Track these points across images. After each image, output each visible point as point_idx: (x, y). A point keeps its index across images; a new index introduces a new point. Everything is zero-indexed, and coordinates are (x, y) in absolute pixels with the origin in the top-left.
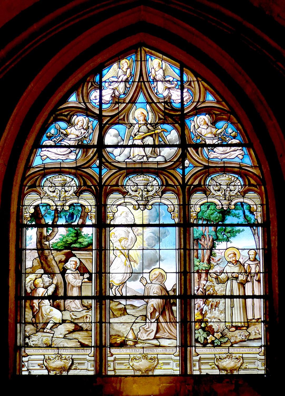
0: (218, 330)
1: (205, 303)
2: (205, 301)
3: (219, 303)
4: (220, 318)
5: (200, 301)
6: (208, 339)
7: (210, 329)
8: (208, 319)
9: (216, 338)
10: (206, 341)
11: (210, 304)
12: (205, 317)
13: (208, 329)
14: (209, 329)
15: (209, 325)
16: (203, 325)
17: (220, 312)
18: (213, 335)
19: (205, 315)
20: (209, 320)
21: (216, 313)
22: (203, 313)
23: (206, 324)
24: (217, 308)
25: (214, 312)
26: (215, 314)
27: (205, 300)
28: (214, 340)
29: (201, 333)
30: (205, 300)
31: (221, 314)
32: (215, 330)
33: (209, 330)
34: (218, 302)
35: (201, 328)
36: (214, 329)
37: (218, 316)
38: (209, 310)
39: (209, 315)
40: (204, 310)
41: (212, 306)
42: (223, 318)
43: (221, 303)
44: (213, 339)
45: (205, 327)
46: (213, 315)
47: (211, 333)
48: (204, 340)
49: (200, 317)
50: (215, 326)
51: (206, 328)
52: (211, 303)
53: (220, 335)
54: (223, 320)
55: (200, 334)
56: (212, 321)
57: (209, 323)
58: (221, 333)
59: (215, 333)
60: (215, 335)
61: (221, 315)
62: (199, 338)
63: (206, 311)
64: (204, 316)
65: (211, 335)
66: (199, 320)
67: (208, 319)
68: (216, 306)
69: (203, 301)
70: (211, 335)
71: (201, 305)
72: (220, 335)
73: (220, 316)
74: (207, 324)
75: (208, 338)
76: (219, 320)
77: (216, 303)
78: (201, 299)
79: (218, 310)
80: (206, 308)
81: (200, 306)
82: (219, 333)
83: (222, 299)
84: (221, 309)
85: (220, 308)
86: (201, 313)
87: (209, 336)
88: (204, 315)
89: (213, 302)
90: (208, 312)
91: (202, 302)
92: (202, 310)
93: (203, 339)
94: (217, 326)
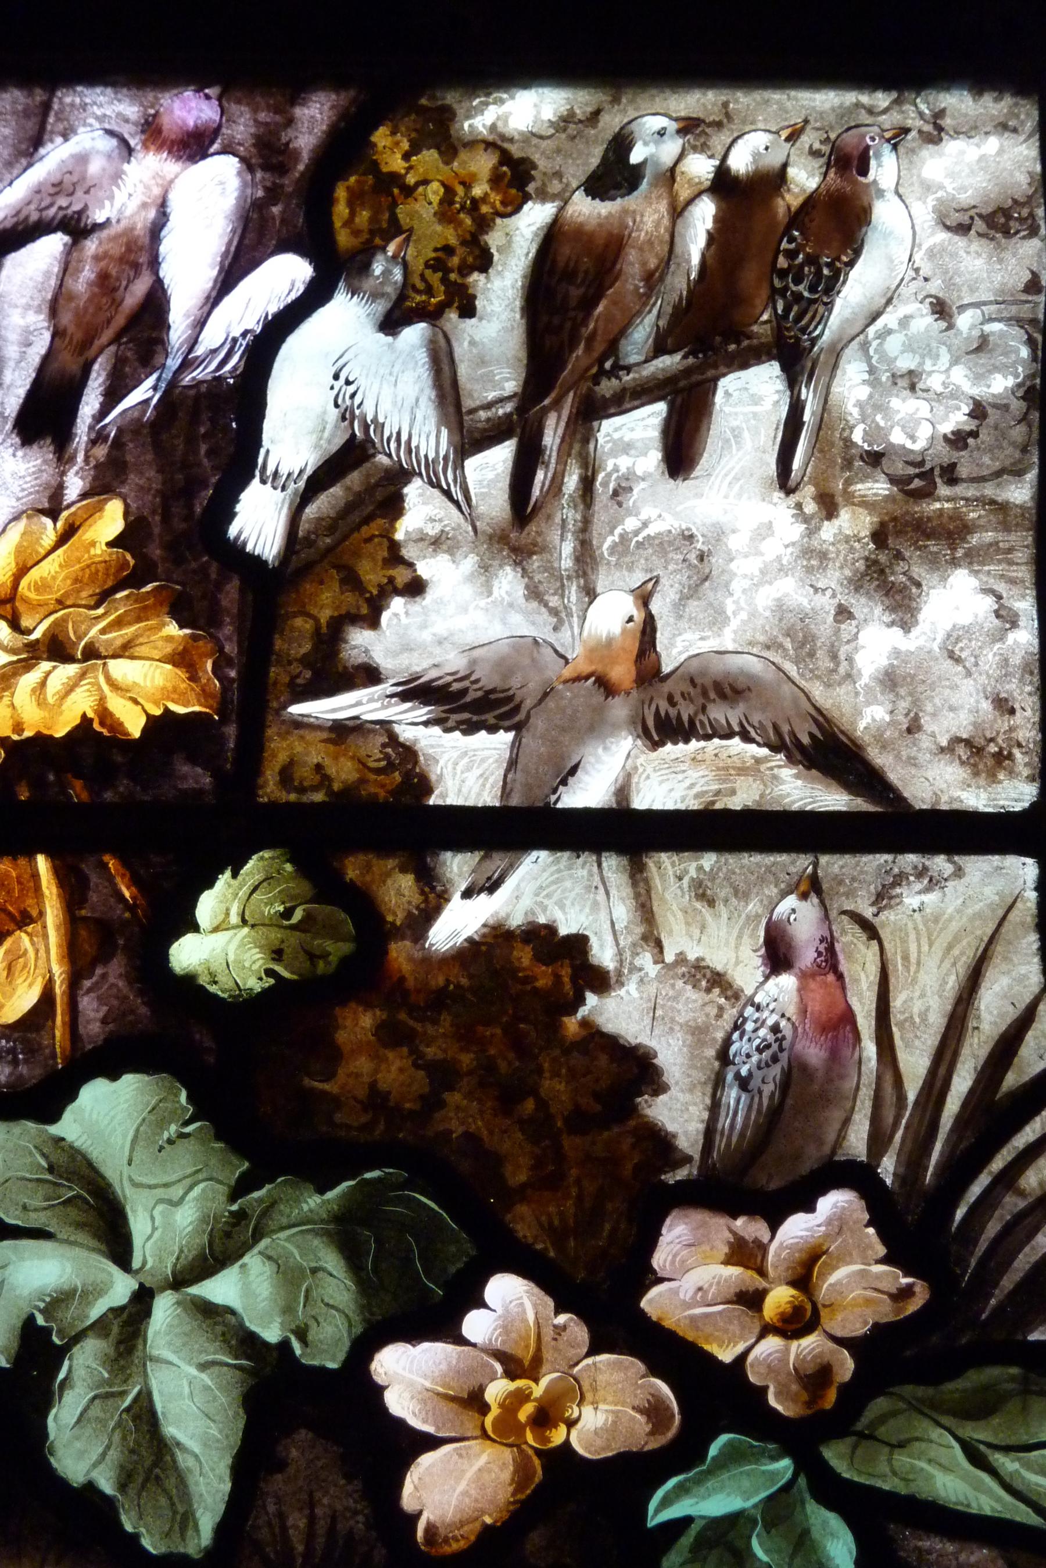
0: (798, 1092)
1: (304, 214)
2: (345, 147)
3: (840, 220)
4: (869, 717)
5: (150, 167)
6: (399, 1403)
7: (507, 1094)
8: (412, 724)
9: (710, 1397)
10: (315, 1488)
11: (535, 216)
12: (336, 675)
13: (395, 1073)
14: (443, 1076)
15: (458, 923)
16: (223, 941)
17: (852, 524)
18: (607, 1300)
19: (327, 600)
20: (467, 768)
21: (721, 532)
22: (260, 520)
23: (363, 907)
24: (750, 399)
25: (659, 508)
26: (698, 560)
27: (313, 118)
28: (633, 1473)
29: (165, 1220)
30: (313, 118)
31: (886, 574)
32: (679, 1113)
33: (462, 1114)
34: (805, 178)
35: (173, 1033)
36: (639, 1070)
37: (799, 637)
38: (471, 441)
39: (454, 611)
40: (293, 432)
41: (568, 287)
42: (960, 706)
43: (886, 213)
44: (609, 1409)
45: (285, 1016)
46: (611, 614)
47: (525, 1224)
48: (251, 1465)
49: (141, 681)
50: (683, 980)
51: (359, 1024)
52: (535, 216)
53: (863, 1284)
54: (981, 755)
55: (117, 1245)
56: (588, 792)
57: (458, 866)
58: (910, 1226)
59: (676, 1235)
60: (690, 1271)
61: (902, 604)
62: (84, 1364)
63: (360, 476)
64: (296, 641)
65: (508, 1294)
66: (92, 745)
67: (412, 724)
68: (713, 330)
69: (266, 156)
70: (508, 1294)
71: (187, 266)
72: (863, 1284)
73: (876, 643)
74: (399, 891)
75: (408, 1375)
76: (831, 752)
77: (704, 215)
78: (189, 108)
79: (810, 460)
80: (342, 371)
81: (156, 303)
82: (834, 1202)
83: (958, 102)
84: (918, 425)
85: (851, 386)
86: (176, 551)
87: (439, 1321)
88: (275, 618)
89: (615, 175)
90: (421, 510)
91: (208, 197)
92: (224, 417)
93: (194, 1405)
94: (746, 969)
